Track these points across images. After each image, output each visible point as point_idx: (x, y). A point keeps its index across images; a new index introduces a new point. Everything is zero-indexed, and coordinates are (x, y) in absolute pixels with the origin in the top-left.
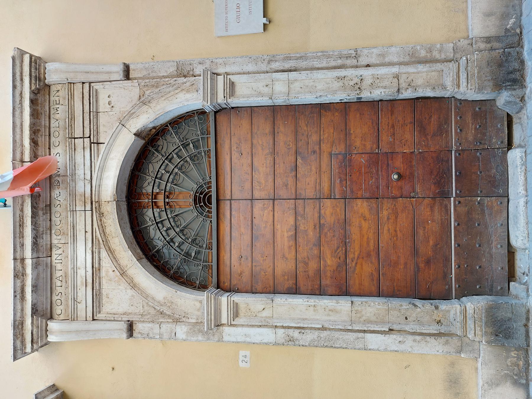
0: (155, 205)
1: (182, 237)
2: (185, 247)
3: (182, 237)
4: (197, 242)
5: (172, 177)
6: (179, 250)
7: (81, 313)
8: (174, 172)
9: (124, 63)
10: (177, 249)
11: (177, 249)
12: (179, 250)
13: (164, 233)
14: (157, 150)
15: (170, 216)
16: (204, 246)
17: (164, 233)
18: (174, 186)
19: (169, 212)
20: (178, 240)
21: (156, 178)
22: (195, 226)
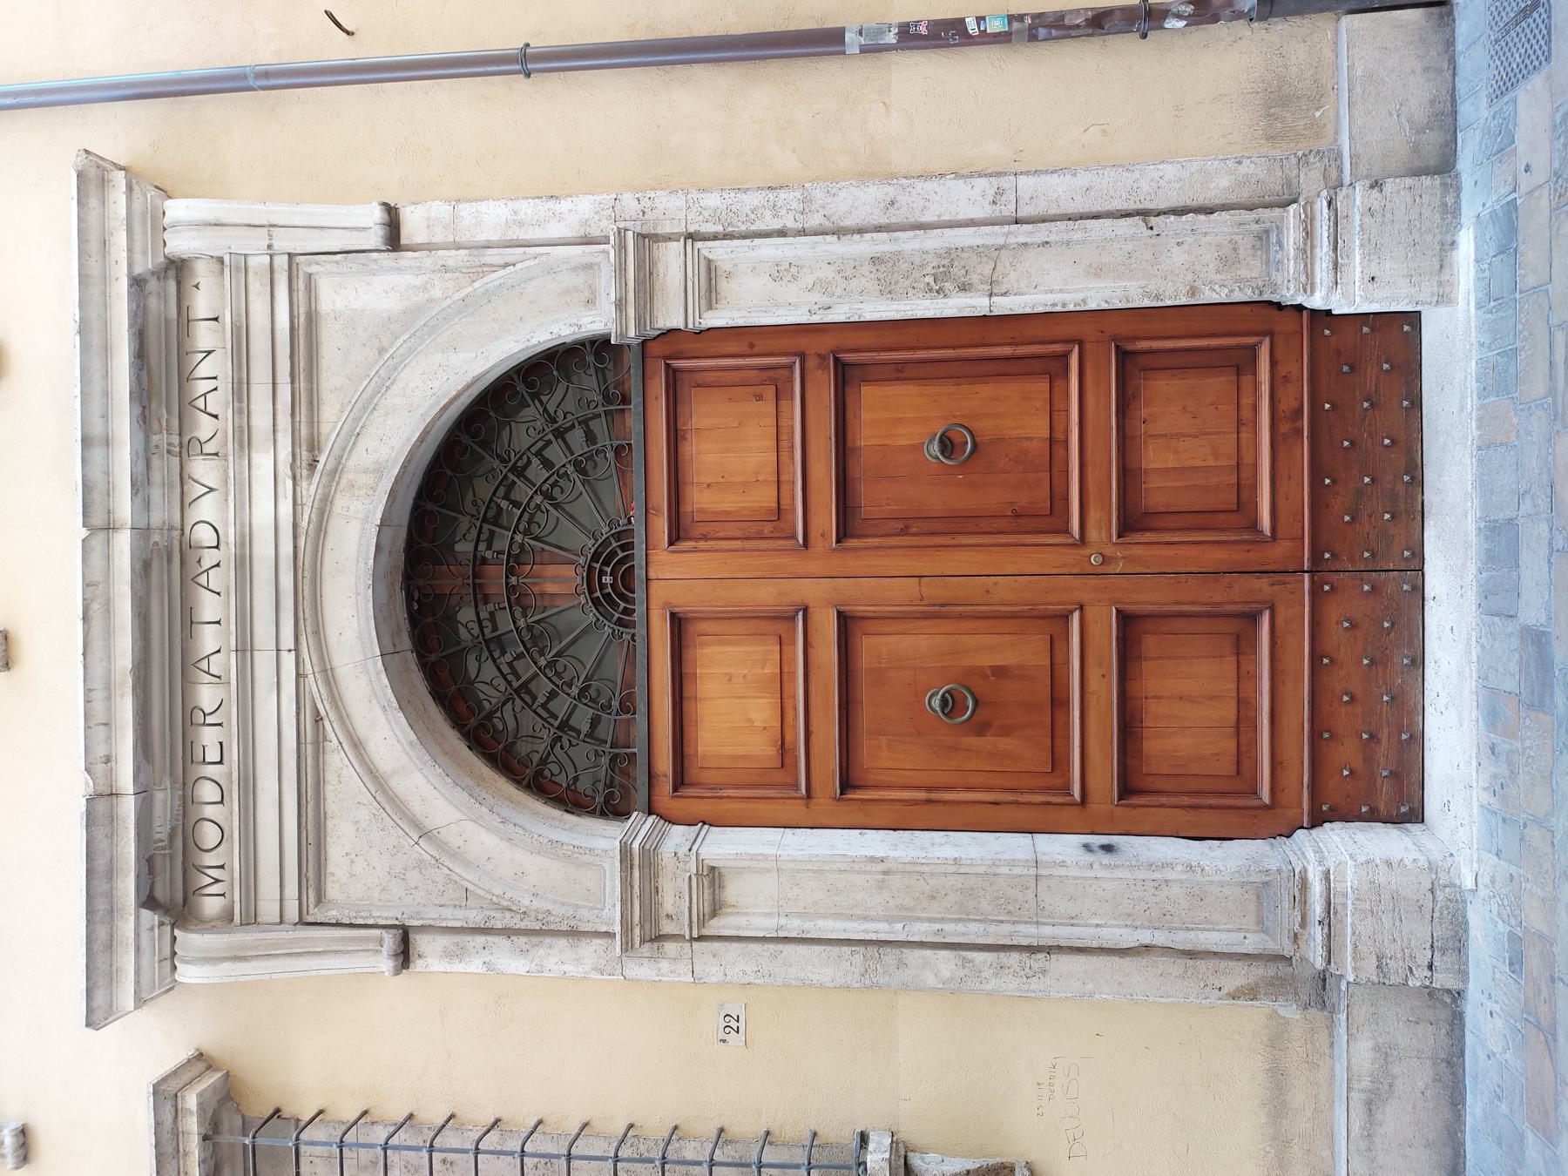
0: (480, 596)
1: (555, 679)
2: (561, 706)
3: (555, 679)
4: (592, 692)
5: (526, 517)
6: (545, 715)
7: (268, 908)
8: (532, 505)
9: (385, 204)
10: (540, 710)
11: (540, 710)
12: (545, 715)
13: (506, 670)
14: (486, 445)
15: (522, 623)
16: (615, 704)
17: (506, 670)
18: (532, 542)
19: (518, 614)
20: (543, 687)
21: (485, 520)
22: (589, 653)
